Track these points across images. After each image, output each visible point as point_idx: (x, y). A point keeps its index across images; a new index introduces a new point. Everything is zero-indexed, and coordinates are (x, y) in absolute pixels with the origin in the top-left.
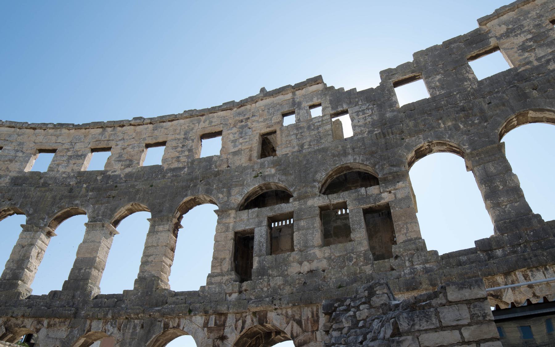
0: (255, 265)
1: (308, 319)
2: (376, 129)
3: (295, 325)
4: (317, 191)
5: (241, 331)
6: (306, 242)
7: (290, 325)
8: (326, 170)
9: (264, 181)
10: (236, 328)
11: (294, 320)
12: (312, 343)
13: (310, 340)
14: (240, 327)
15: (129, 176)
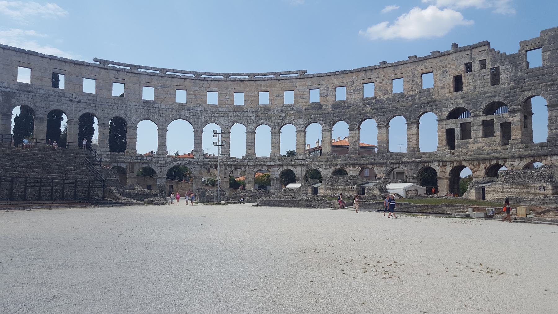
0: (456, 144)
1: (477, 164)
2: (512, 82)
3: (472, 166)
4: (481, 113)
5: (453, 167)
6: (476, 135)
7: (470, 166)
8: (486, 104)
9: (458, 106)
10: (450, 166)
11: (472, 164)
12: (478, 172)
13: (477, 171)
14: (452, 166)
15: (389, 100)
